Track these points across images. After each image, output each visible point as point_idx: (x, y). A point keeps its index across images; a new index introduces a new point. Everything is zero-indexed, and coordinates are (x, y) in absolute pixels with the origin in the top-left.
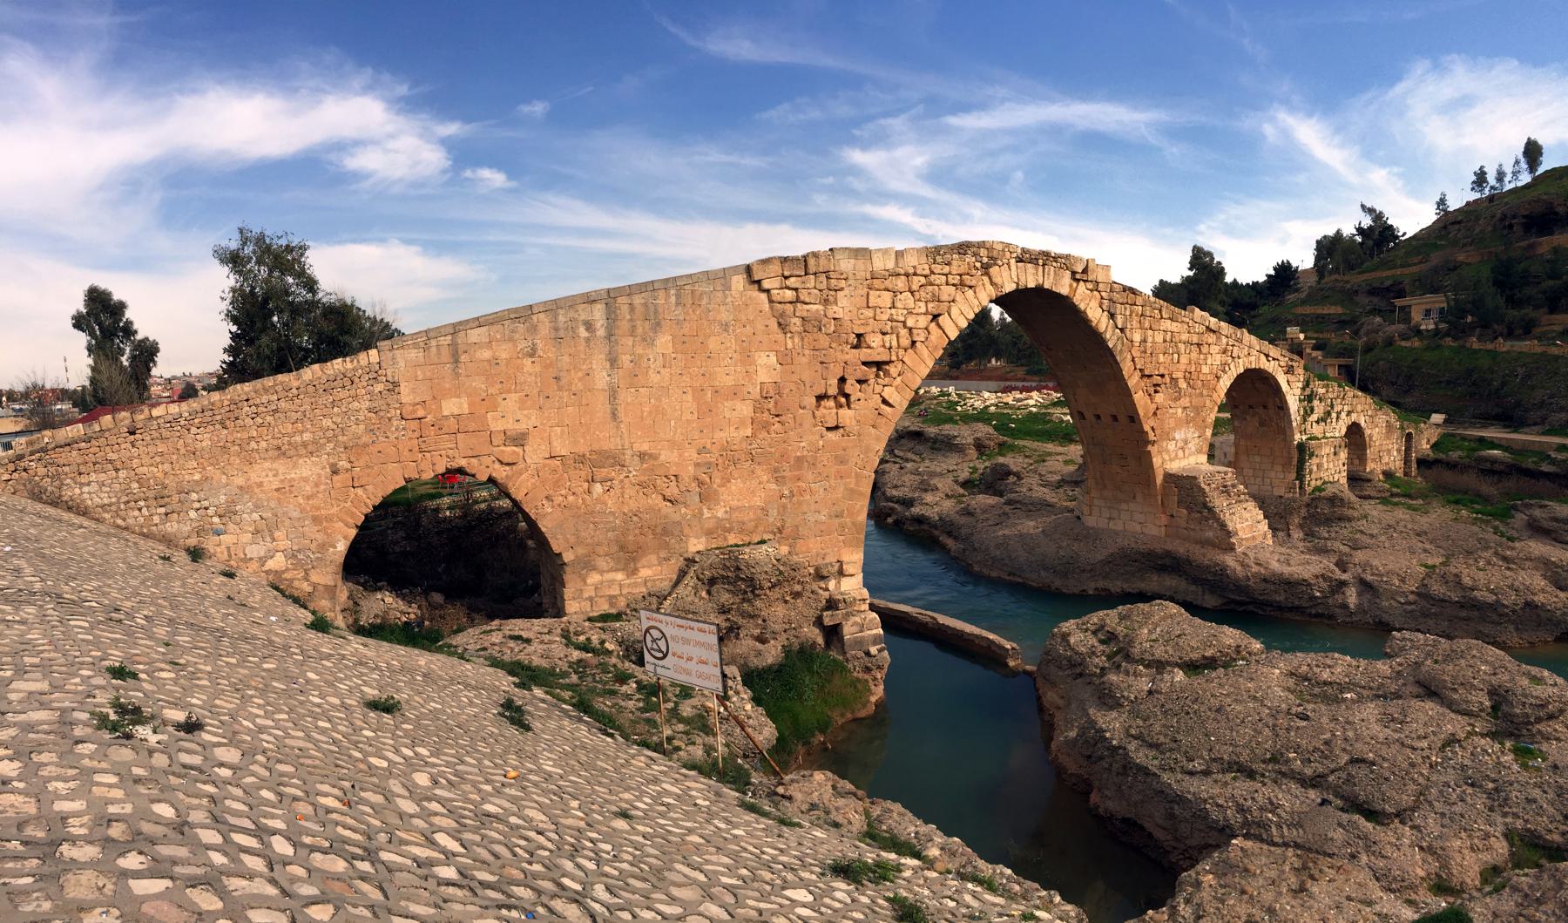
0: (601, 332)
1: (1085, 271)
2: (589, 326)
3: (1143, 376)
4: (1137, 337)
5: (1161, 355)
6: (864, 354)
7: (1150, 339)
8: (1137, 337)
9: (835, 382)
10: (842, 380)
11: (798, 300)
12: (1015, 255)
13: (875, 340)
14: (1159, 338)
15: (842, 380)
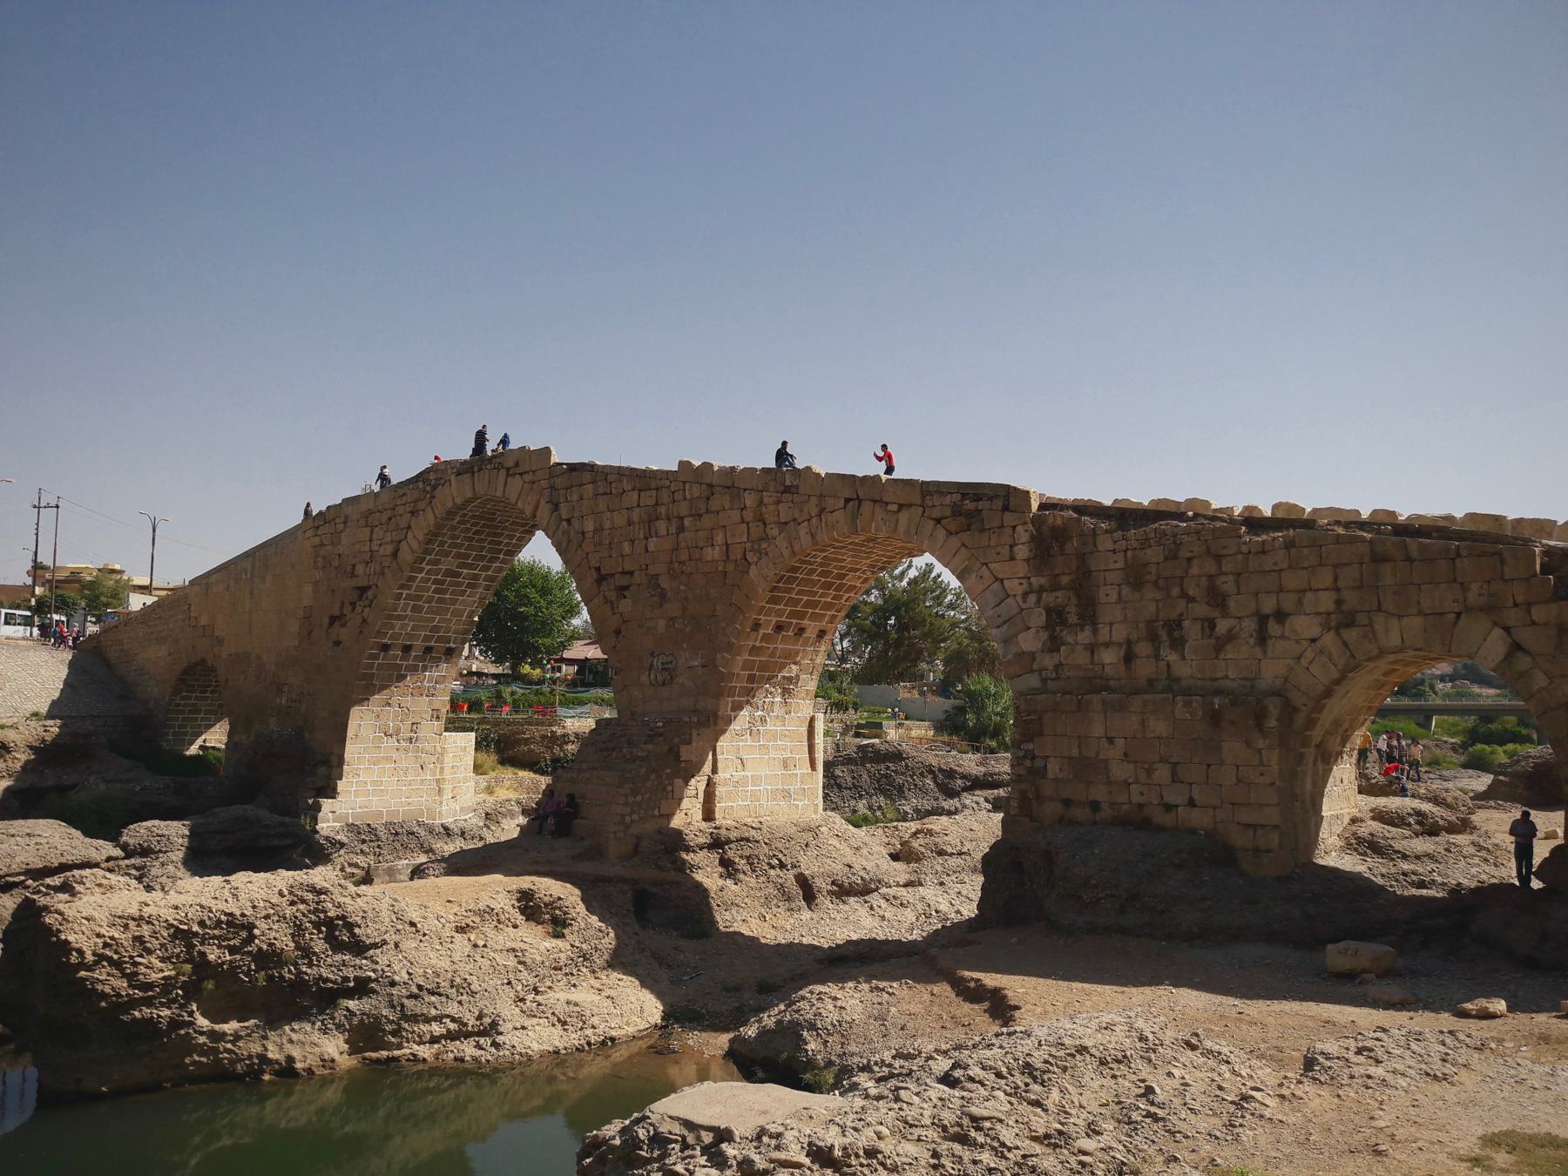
0: (249, 576)
1: (517, 465)
2: (246, 570)
3: (601, 579)
4: (589, 526)
5: (626, 544)
6: (355, 583)
7: (607, 524)
8: (589, 526)
9: (337, 605)
10: (343, 603)
11: (322, 545)
12: (455, 470)
13: (360, 569)
14: (620, 519)
15: (343, 603)
